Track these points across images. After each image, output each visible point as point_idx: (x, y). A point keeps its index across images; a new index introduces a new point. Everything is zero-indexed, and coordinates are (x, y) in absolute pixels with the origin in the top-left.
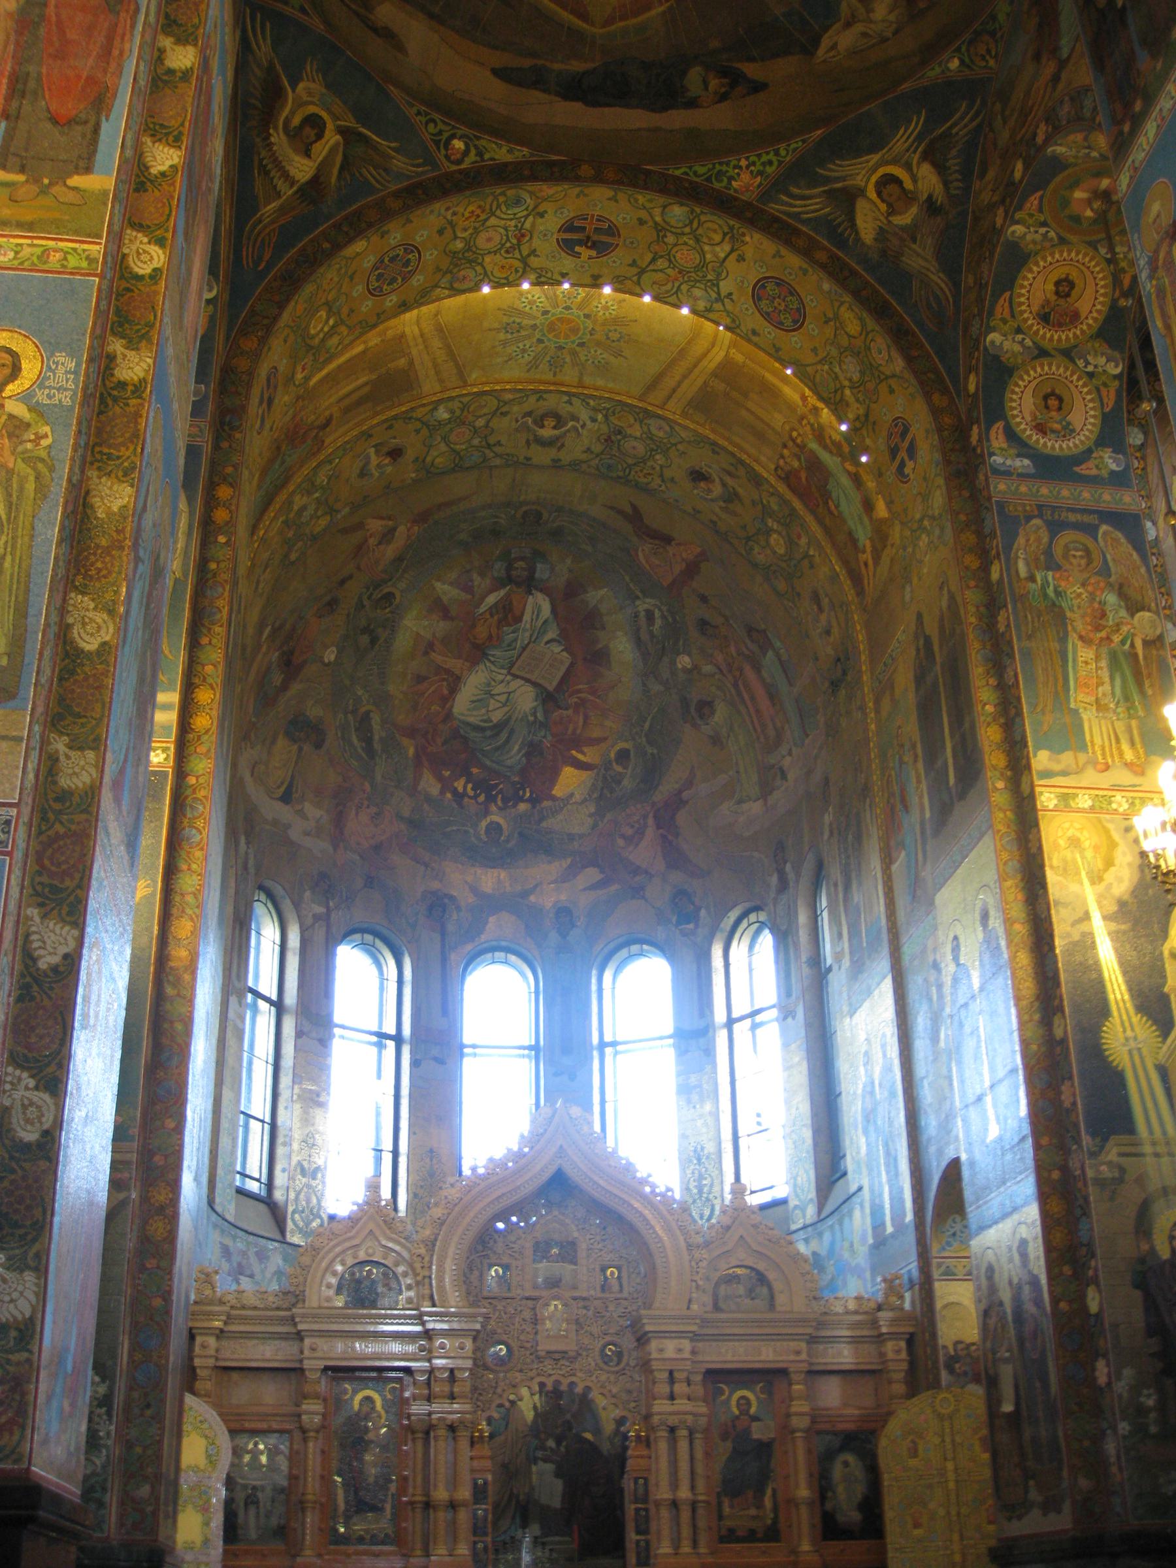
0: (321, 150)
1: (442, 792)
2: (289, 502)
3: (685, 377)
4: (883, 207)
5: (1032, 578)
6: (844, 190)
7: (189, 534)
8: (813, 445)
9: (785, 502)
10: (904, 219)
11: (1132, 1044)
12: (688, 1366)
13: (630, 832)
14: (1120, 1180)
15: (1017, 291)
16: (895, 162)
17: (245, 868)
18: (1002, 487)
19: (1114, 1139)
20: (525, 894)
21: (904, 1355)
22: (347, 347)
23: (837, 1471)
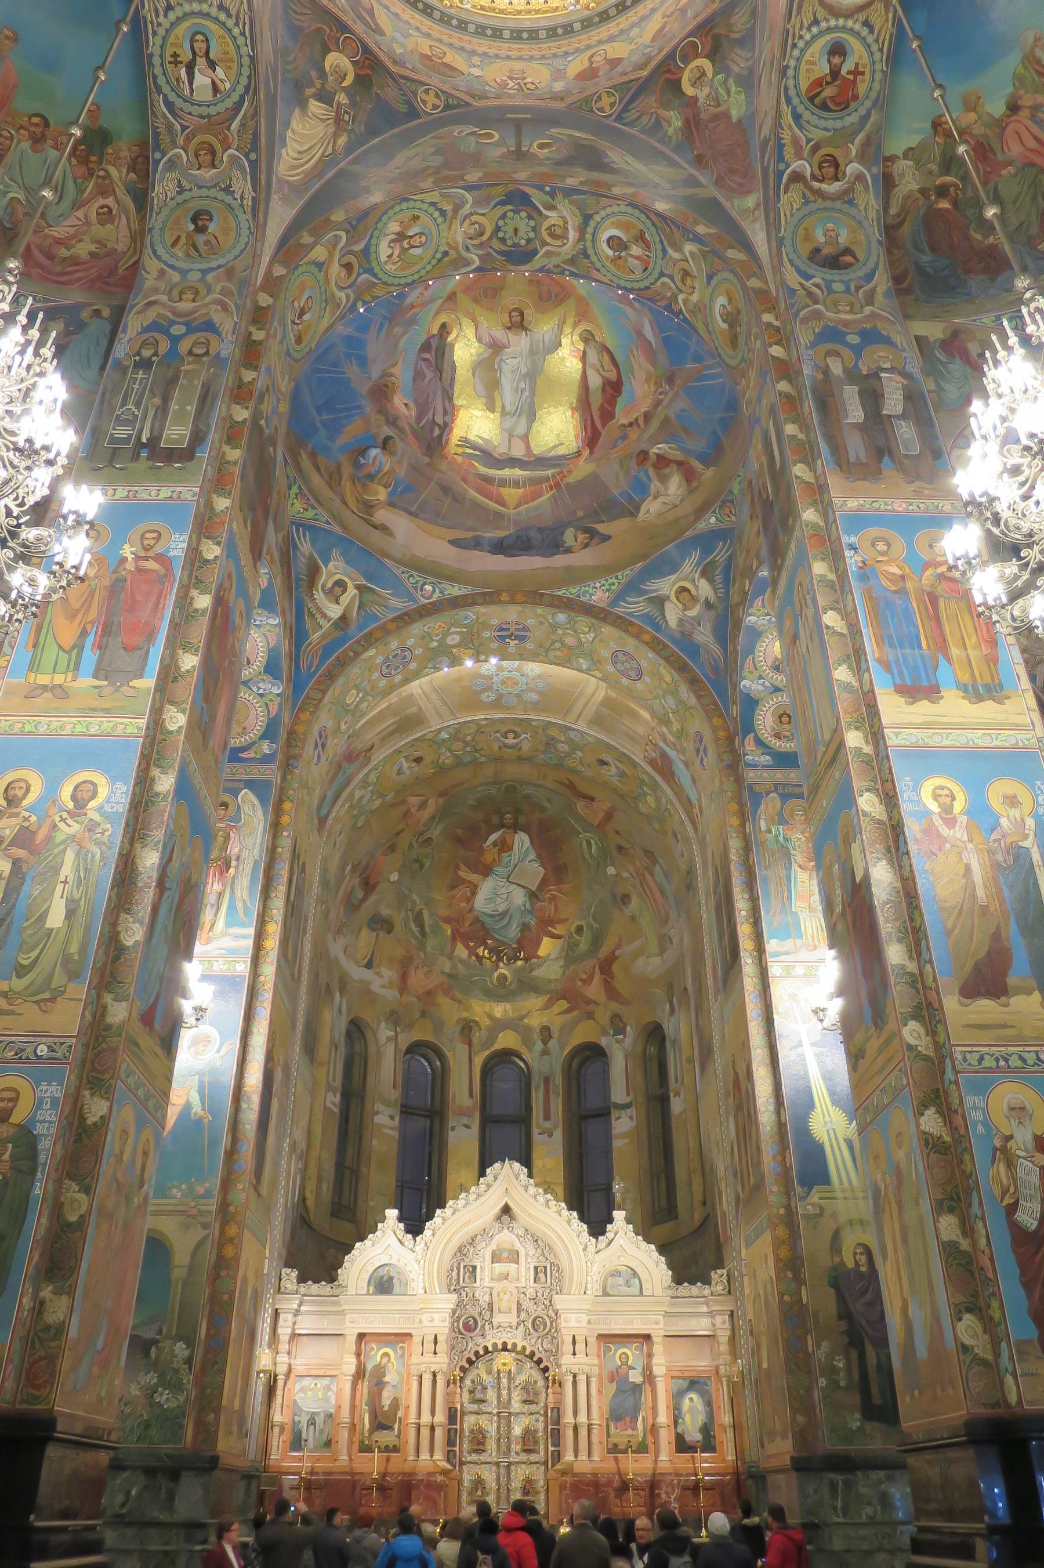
0: (345, 599)
1: (470, 956)
2: (351, 795)
3: (585, 706)
4: (681, 606)
5: (769, 831)
6: (657, 597)
7: (264, 833)
8: (662, 745)
9: (652, 778)
10: (693, 612)
11: (829, 1126)
12: (585, 1332)
13: (584, 976)
14: (821, 1214)
15: (757, 653)
16: (682, 580)
17: (340, 1011)
18: (751, 775)
19: (816, 1188)
20: (522, 1018)
21: (727, 1325)
22: (373, 708)
23: (686, 1404)
